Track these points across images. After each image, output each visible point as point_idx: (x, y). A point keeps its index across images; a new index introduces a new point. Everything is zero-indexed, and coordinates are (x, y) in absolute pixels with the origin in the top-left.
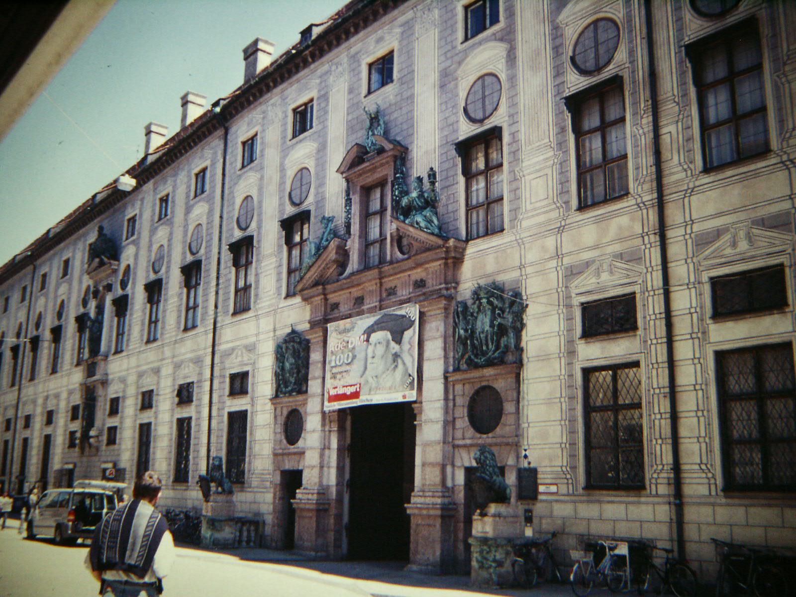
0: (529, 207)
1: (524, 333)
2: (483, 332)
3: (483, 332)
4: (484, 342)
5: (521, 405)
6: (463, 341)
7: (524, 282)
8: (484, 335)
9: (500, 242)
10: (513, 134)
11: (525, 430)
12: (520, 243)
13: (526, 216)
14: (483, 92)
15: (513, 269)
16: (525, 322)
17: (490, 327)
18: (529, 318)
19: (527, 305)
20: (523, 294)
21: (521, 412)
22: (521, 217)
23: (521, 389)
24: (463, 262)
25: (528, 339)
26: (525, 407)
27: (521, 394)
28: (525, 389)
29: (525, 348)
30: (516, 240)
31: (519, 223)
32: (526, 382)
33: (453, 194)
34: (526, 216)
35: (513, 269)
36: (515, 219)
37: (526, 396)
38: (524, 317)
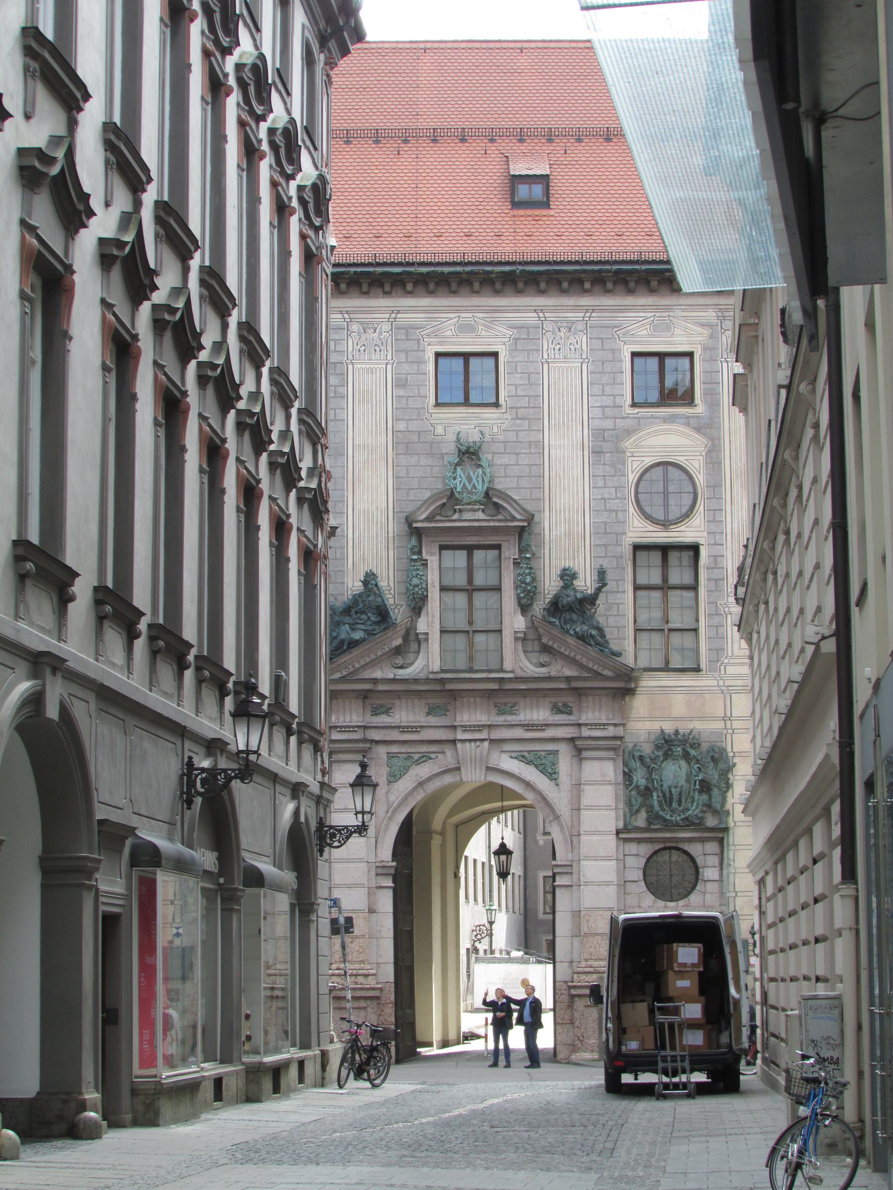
0: (736, 653)
1: (729, 794)
2: (676, 787)
3: (676, 787)
4: (675, 798)
5: (725, 872)
6: (647, 792)
7: (729, 736)
8: (678, 790)
9: (693, 683)
10: (715, 557)
11: (731, 899)
12: (727, 692)
13: (731, 661)
14: (665, 487)
15: (714, 718)
16: (730, 782)
17: (686, 781)
18: (737, 778)
19: (734, 765)
20: (729, 749)
21: (725, 879)
22: (726, 661)
23: (725, 854)
24: (634, 694)
25: (733, 801)
26: (732, 876)
27: (726, 860)
28: (731, 856)
29: (731, 812)
30: (718, 686)
31: (722, 667)
32: (732, 847)
33: (618, 605)
34: (731, 661)
35: (714, 718)
36: (718, 661)
37: (732, 863)
38: (730, 776)
